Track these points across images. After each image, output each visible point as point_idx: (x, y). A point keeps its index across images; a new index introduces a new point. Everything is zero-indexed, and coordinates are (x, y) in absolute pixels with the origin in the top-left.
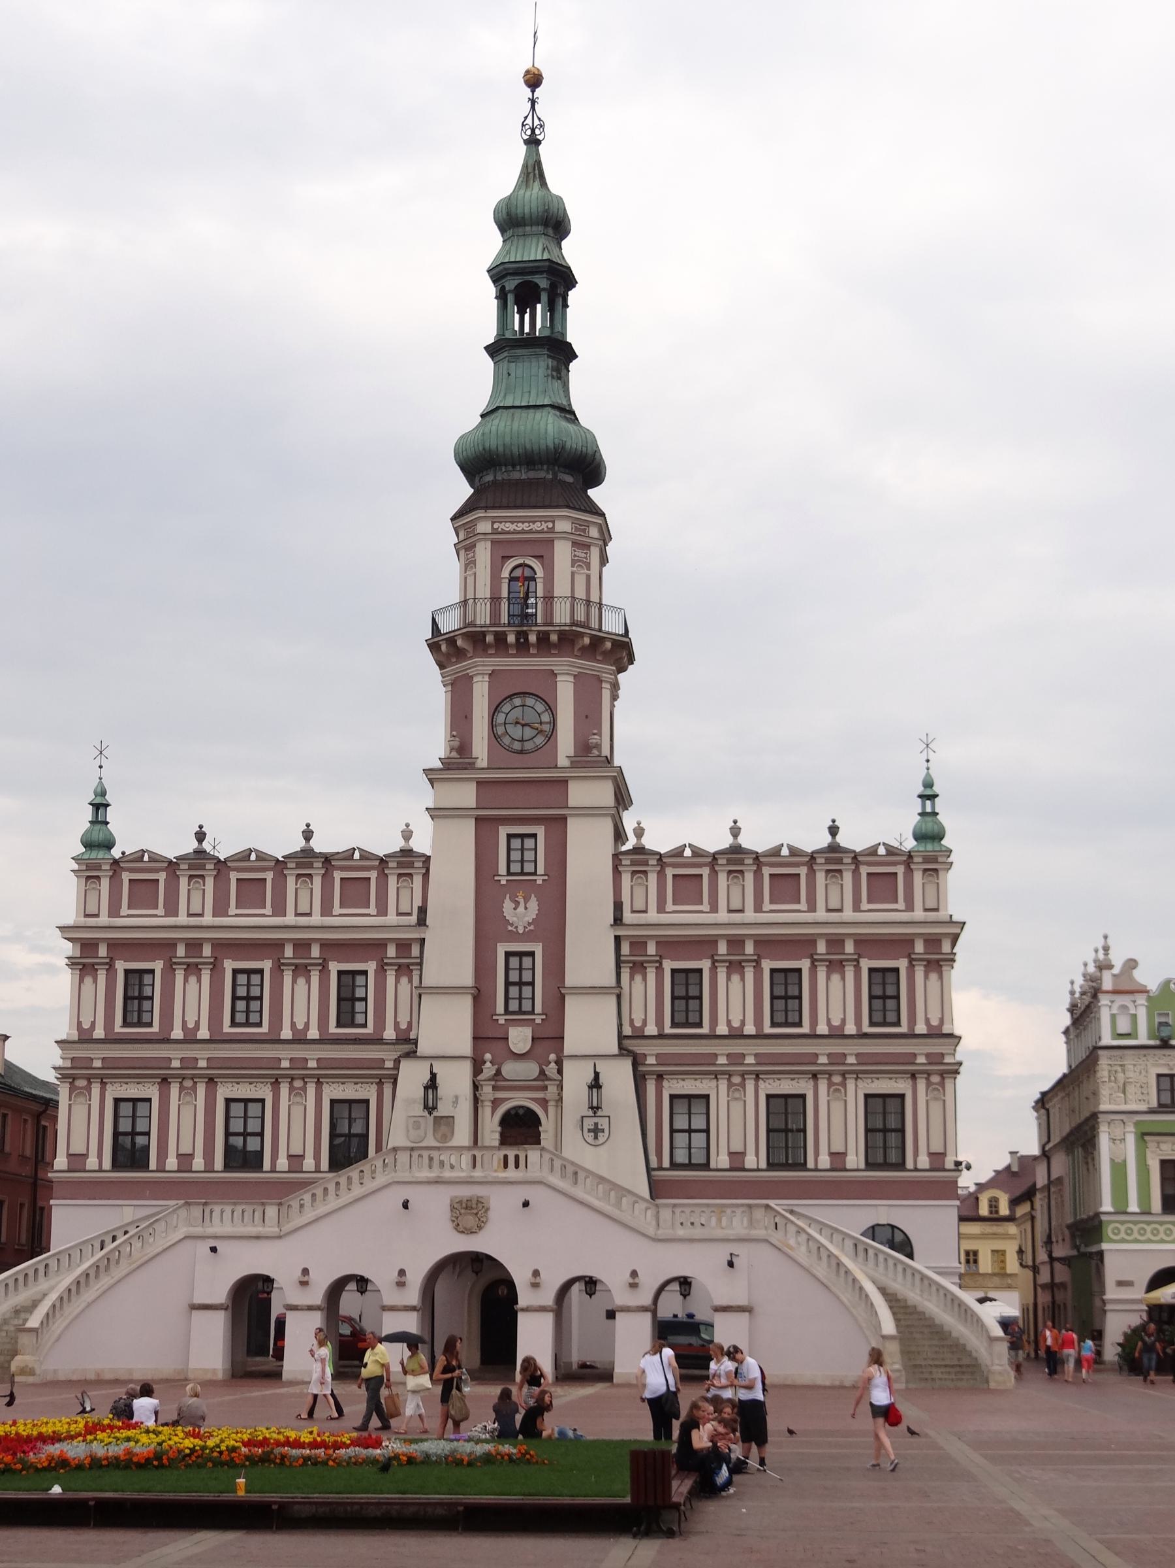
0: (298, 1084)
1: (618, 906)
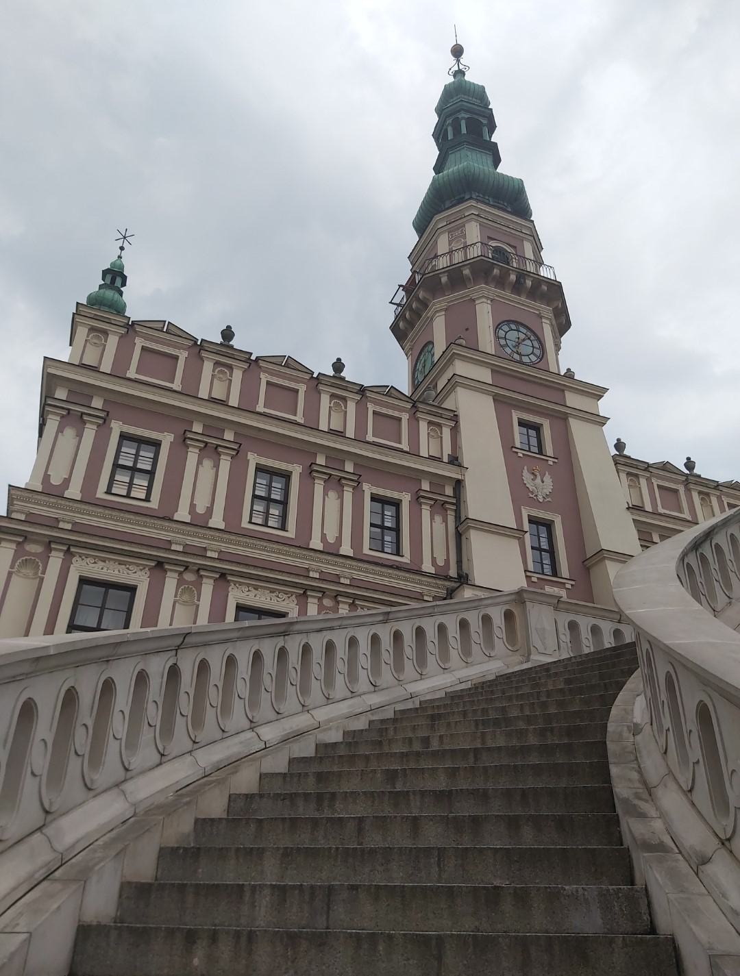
0: (327, 602)
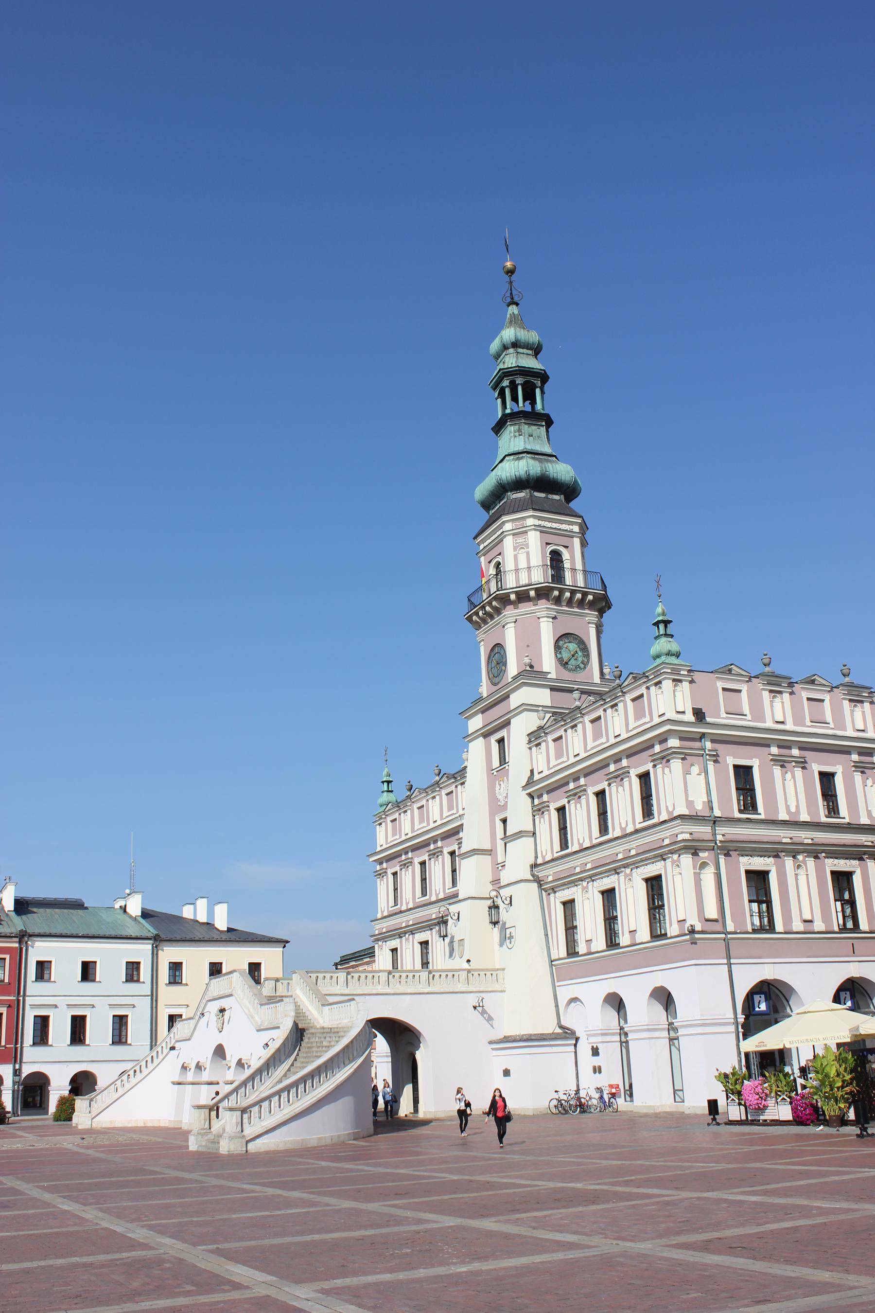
1: (532, 771)
